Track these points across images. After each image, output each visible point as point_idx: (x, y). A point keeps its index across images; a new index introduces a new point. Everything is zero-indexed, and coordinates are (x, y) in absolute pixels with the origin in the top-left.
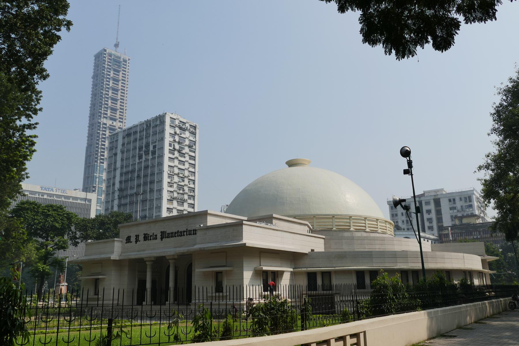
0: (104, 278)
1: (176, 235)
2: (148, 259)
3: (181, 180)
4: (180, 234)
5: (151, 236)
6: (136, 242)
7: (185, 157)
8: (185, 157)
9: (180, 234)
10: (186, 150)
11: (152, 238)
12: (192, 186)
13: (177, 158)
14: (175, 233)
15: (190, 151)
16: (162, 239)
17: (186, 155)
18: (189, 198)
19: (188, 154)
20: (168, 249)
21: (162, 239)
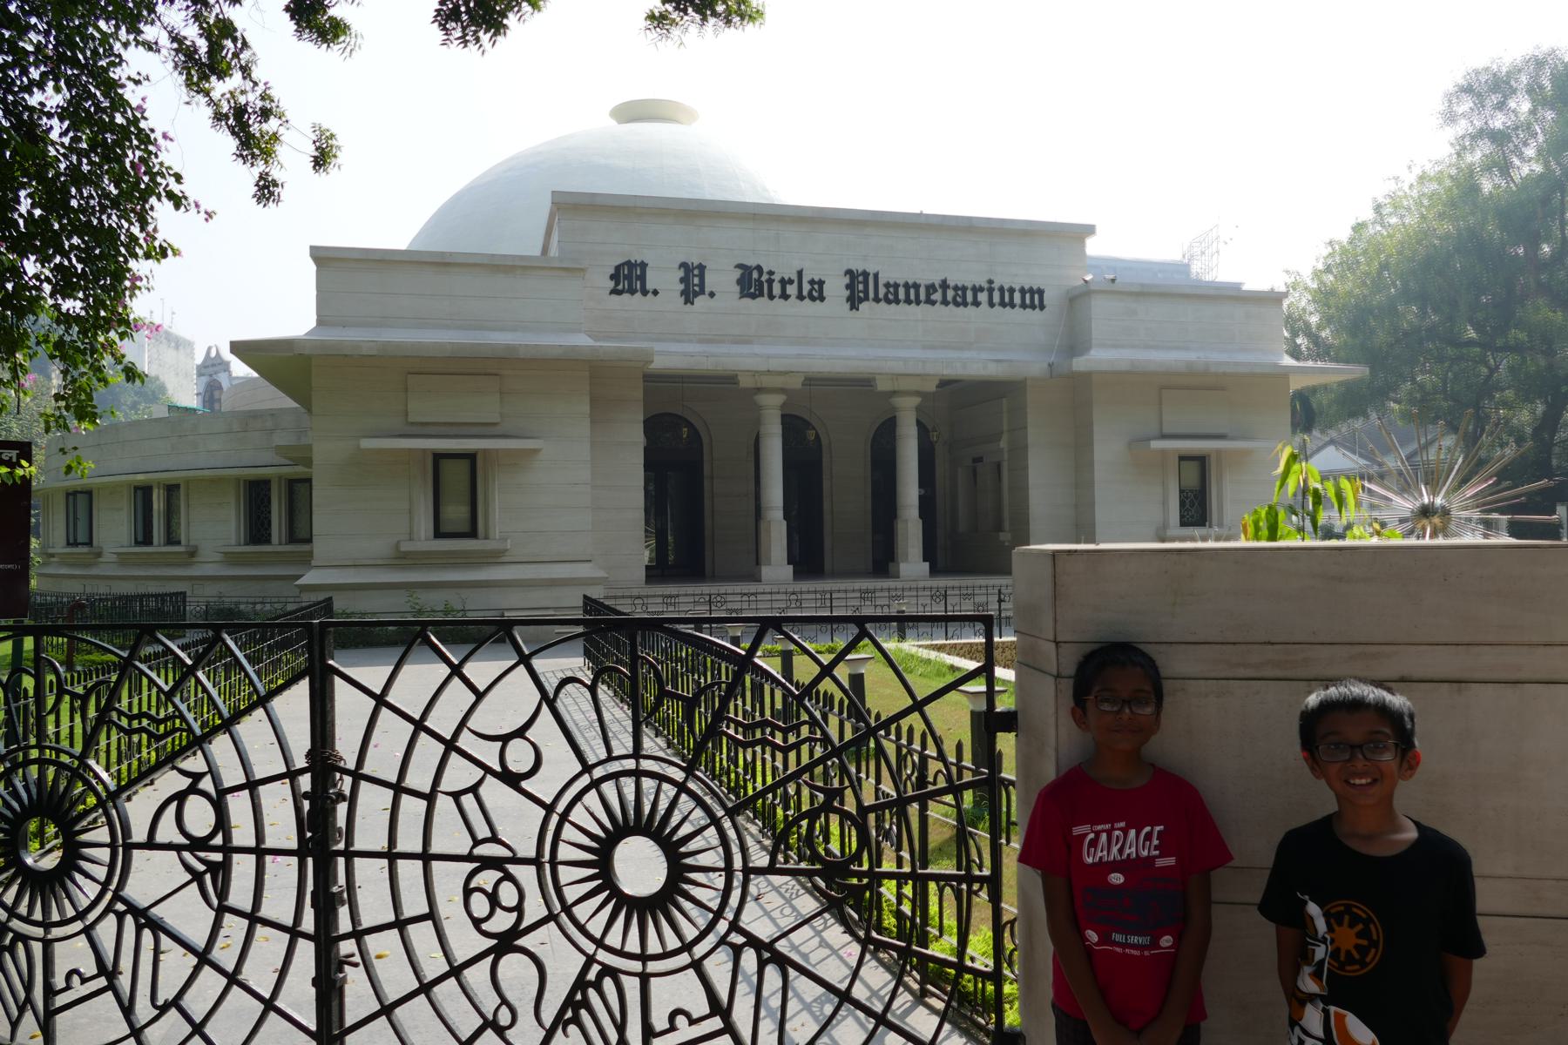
0: (536, 451)
1: (937, 296)
2: (778, 382)
4: (961, 296)
5: (784, 283)
6: (689, 296)
9: (961, 296)
11: (792, 290)
14: (931, 288)
16: (854, 302)
20: (906, 350)
21: (854, 302)
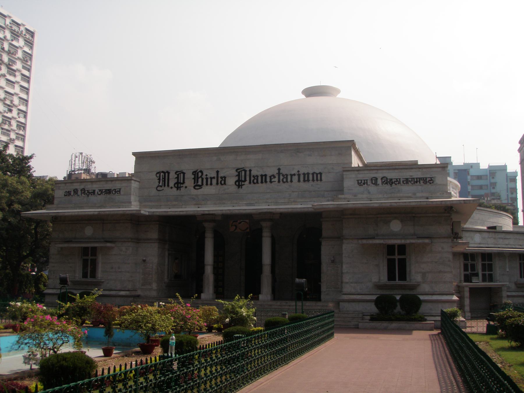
3: (7, 110)
7: (15, 76)
8: (15, 76)
10: (18, 66)
12: (22, 120)
13: (5, 76)
15: (24, 67)
17: (17, 74)
18: (17, 138)
19: (20, 71)
